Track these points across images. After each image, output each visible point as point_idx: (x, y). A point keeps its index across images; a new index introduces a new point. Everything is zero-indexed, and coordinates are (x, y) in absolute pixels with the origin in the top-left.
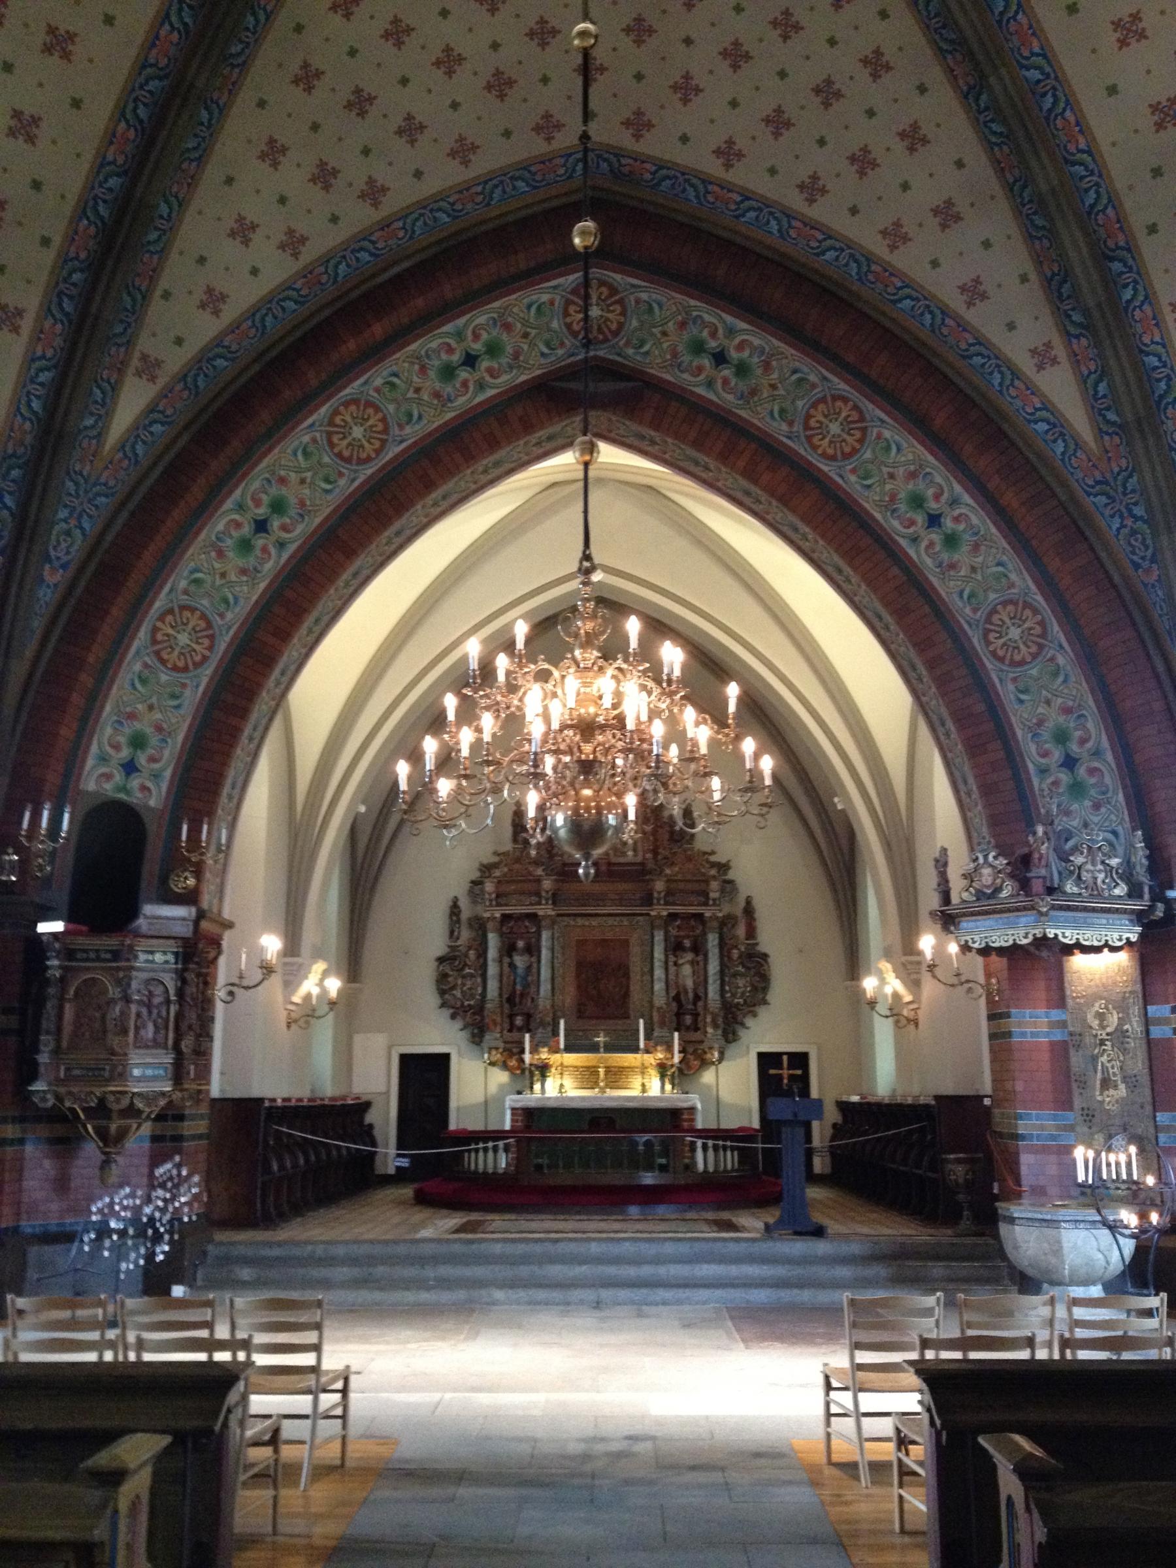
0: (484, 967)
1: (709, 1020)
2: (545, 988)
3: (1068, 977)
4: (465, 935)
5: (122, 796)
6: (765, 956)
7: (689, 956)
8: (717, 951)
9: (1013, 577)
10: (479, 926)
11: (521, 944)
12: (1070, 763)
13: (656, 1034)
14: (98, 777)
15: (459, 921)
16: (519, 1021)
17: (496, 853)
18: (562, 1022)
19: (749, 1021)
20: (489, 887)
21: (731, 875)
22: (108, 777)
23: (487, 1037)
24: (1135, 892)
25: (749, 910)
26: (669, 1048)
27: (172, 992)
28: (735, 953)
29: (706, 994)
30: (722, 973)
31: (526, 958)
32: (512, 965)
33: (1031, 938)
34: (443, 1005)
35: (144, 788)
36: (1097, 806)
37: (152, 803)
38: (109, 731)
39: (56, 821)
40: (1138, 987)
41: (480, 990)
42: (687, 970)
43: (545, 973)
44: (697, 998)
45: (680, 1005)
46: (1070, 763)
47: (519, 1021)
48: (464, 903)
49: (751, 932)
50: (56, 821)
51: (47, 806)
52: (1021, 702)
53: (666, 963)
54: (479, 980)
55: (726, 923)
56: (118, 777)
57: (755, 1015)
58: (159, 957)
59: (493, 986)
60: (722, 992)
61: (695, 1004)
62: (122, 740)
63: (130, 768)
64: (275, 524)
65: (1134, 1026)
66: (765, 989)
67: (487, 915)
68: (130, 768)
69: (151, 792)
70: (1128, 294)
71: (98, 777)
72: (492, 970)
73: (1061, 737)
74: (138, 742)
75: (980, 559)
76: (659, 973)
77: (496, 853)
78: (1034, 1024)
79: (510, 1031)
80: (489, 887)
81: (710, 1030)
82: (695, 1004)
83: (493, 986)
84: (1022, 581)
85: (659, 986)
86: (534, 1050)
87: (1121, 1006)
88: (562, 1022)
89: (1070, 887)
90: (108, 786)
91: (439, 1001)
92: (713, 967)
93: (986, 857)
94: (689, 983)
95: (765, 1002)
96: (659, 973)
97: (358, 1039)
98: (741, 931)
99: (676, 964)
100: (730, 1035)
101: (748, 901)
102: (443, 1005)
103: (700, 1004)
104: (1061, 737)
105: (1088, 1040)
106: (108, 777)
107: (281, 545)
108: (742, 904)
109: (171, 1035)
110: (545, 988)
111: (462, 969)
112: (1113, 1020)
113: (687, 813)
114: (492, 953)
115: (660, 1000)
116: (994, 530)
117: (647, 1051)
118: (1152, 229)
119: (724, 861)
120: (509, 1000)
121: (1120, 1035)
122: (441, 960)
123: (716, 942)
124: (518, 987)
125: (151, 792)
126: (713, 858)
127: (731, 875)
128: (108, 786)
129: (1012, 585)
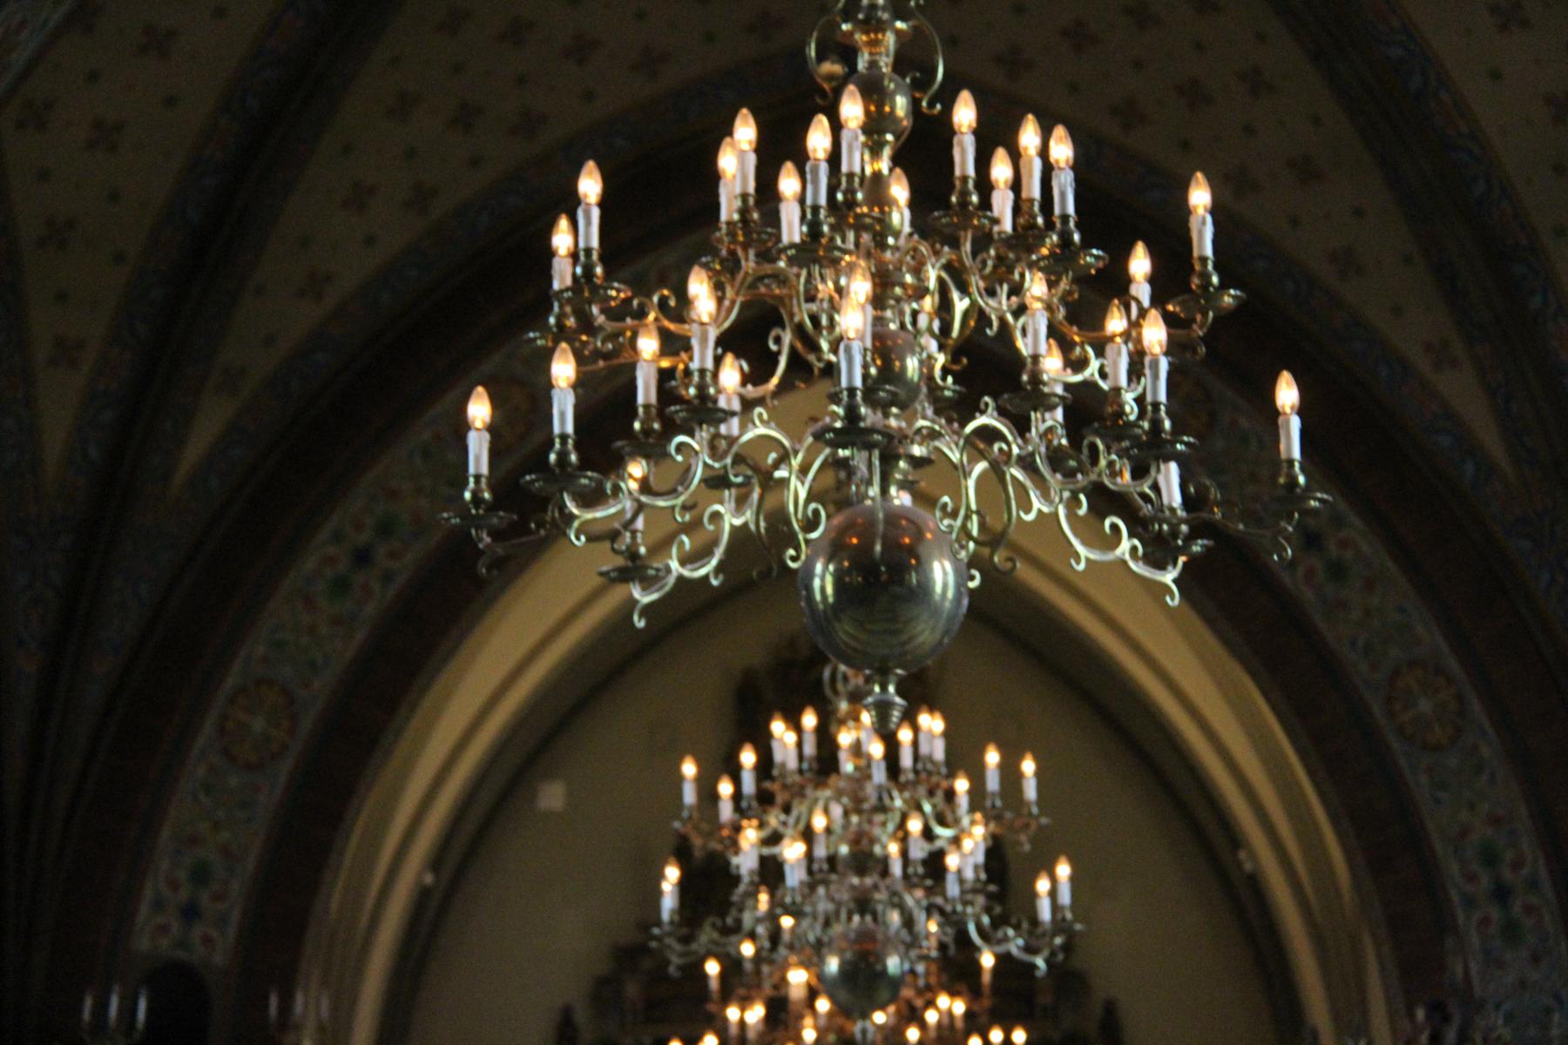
5: (181, 954)
20: (632, 990)
22: (164, 929)
35: (207, 940)
36: (1536, 959)
37: (219, 959)
39: (129, 1010)
46: (1501, 894)
48: (581, 1017)
50: (129, 1010)
51: (117, 988)
52: (1437, 801)
56: (176, 926)
62: (182, 875)
63: (190, 913)
68: (190, 913)
69: (215, 946)
70: (1536, 301)
71: (152, 933)
73: (1490, 857)
74: (201, 875)
80: (632, 990)
84: (1430, 637)
101: (1110, 1008)
104: (1490, 857)
106: (164, 929)
107: (387, 577)
116: (1390, 564)
125: (215, 946)
128: (164, 943)
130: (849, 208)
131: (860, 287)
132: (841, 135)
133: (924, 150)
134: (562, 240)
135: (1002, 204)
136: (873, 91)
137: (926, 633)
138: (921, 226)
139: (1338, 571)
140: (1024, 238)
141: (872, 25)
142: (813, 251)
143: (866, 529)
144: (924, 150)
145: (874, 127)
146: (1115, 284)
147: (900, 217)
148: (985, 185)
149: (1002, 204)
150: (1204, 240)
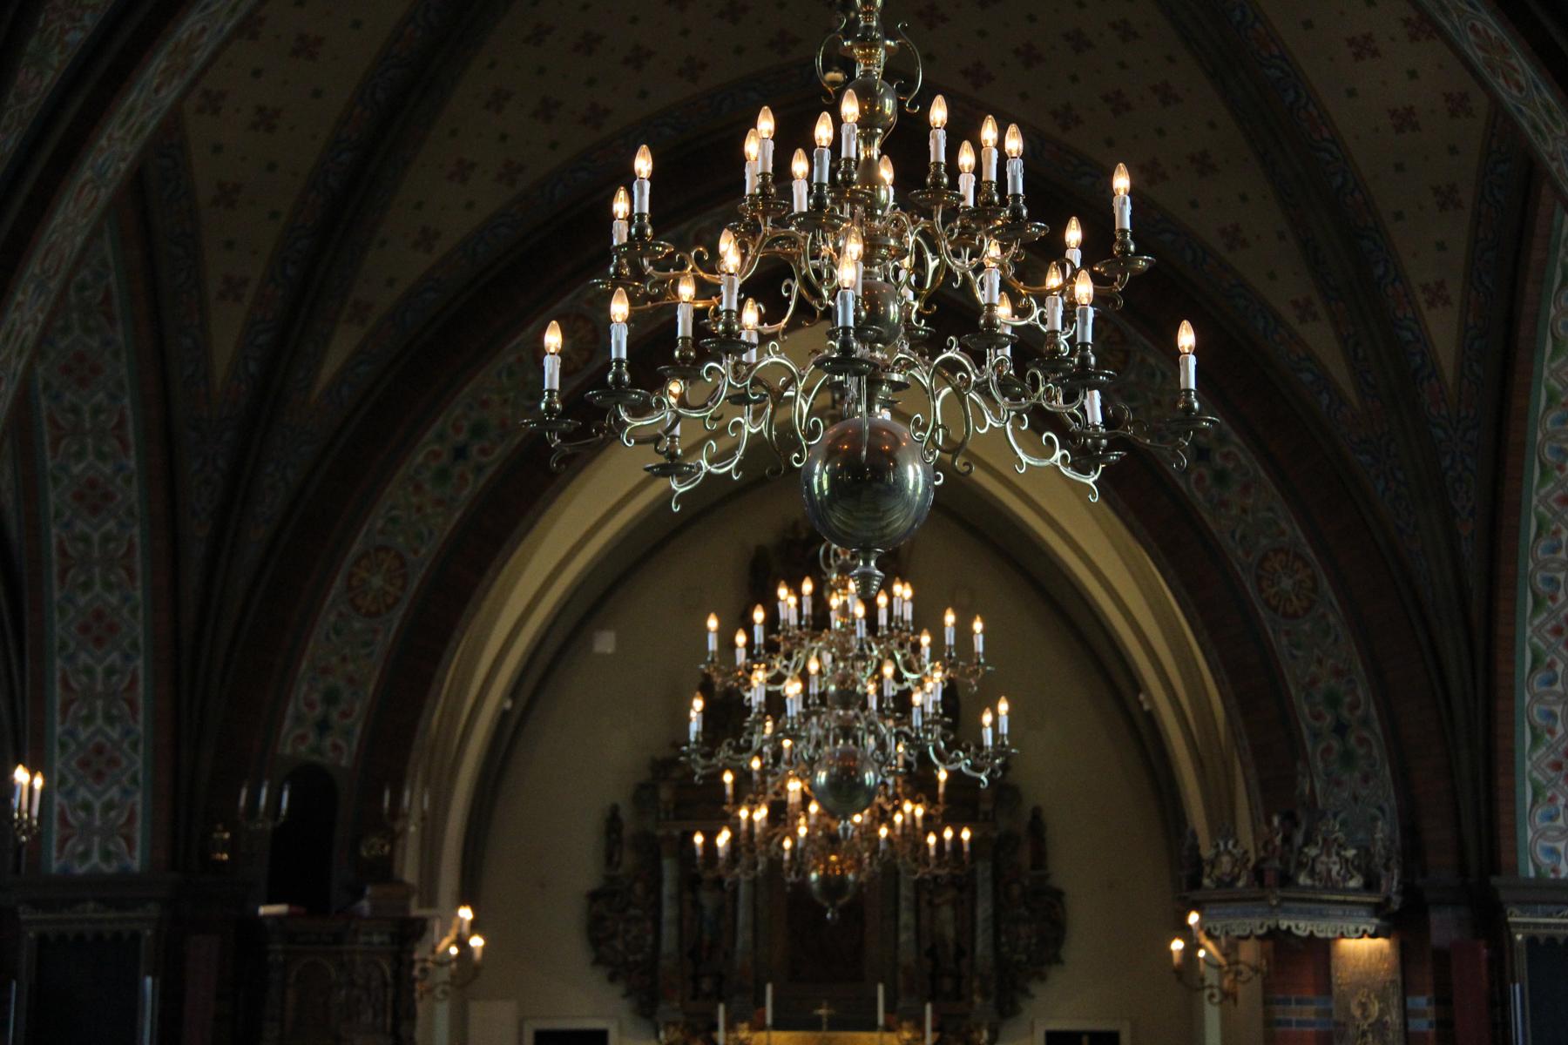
0: (657, 906)
1: (976, 984)
2: (744, 937)
3: (1334, 962)
4: (628, 859)
5: (315, 758)
6: (1059, 894)
8: (989, 886)
9: (1283, 525)
10: (651, 850)
12: (1341, 729)
13: (901, 1005)
14: (293, 741)
16: (706, 985)
18: (769, 988)
20: (665, 793)
23: (663, 1007)
24: (1370, 885)
25: (1037, 825)
26: (919, 1026)
27: (388, 973)
28: (1016, 890)
29: (973, 949)
30: (996, 917)
32: (696, 905)
33: (1265, 929)
35: (336, 747)
36: (1366, 779)
37: (344, 762)
38: (304, 688)
39: (275, 800)
40: (1398, 977)
41: (650, 938)
42: (946, 913)
43: (743, 916)
44: (960, 953)
46: (1341, 729)
47: (706, 985)
48: (626, 813)
49: (1040, 858)
50: (275, 800)
51: (266, 783)
52: (1294, 657)
53: (917, 901)
54: (649, 925)
56: (312, 738)
57: (1043, 978)
58: (376, 939)
59: (669, 934)
60: (996, 946)
62: (316, 696)
64: (474, 450)
65: (1393, 1018)
67: (661, 833)
68: (323, 726)
69: (342, 752)
70: (1379, 271)
71: (293, 741)
72: (668, 912)
74: (331, 698)
75: (1250, 501)
76: (906, 917)
78: (1303, 1013)
79: (694, 998)
80: (665, 793)
81: (978, 999)
83: (669, 934)
85: (903, 937)
86: (731, 1027)
87: (1382, 997)
88: (769, 988)
89: (1303, 879)
90: (302, 748)
92: (984, 909)
93: (1226, 845)
94: (950, 932)
95: (1057, 960)
96: (906, 917)
97: (477, 1010)
98: (1025, 856)
99: (930, 903)
100: (1007, 1006)
101: (1037, 814)
104: (1333, 700)
105: (1351, 1031)
107: (480, 469)
108: (1028, 818)
109: (389, 1021)
110: (744, 937)
112: (1375, 1009)
114: (668, 888)
115: (907, 955)
116: (1262, 474)
117: (888, 1028)
118: (1399, 216)
121: (1380, 1026)
122: (593, 896)
123: (988, 874)
124: (707, 937)
125: (342, 752)
128: (302, 748)
129: (1283, 533)
130: (845, 187)
131: (854, 248)
132: (842, 126)
133: (906, 142)
134: (620, 206)
135: (967, 184)
136: (867, 94)
137: (900, 521)
138: (902, 200)
139: (1221, 477)
140: (984, 211)
141: (867, 42)
142: (818, 219)
143: (856, 438)
144: (906, 142)
145: (867, 122)
146: (1053, 250)
147: (887, 194)
148: (954, 170)
149: (967, 184)
150: (1124, 216)
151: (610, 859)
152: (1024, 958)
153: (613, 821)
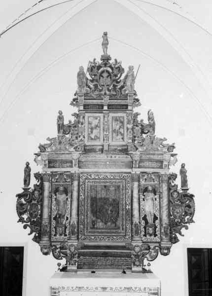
0: (42, 200)
7: (151, 195)
11: (61, 188)
15: (29, 175)
17: (48, 139)
19: (183, 230)
21: (175, 152)
25: (183, 172)
28: (175, 195)
31: (64, 196)
34: (20, 221)
44: (155, 218)
45: (147, 222)
49: (184, 182)
53: (139, 199)
55: (173, 177)
60: (169, 215)
61: (154, 222)
66: (192, 214)
77: (48, 139)
82: (154, 222)
91: (18, 218)
98: (178, 182)
101: (183, 166)
102: (20, 221)
103: (157, 222)
111: (31, 201)
113: (150, 118)
119: (171, 144)
120: (55, 219)
126: (165, 143)
127: (175, 152)
151: (27, 181)
152: (179, 220)
153: (28, 170)
